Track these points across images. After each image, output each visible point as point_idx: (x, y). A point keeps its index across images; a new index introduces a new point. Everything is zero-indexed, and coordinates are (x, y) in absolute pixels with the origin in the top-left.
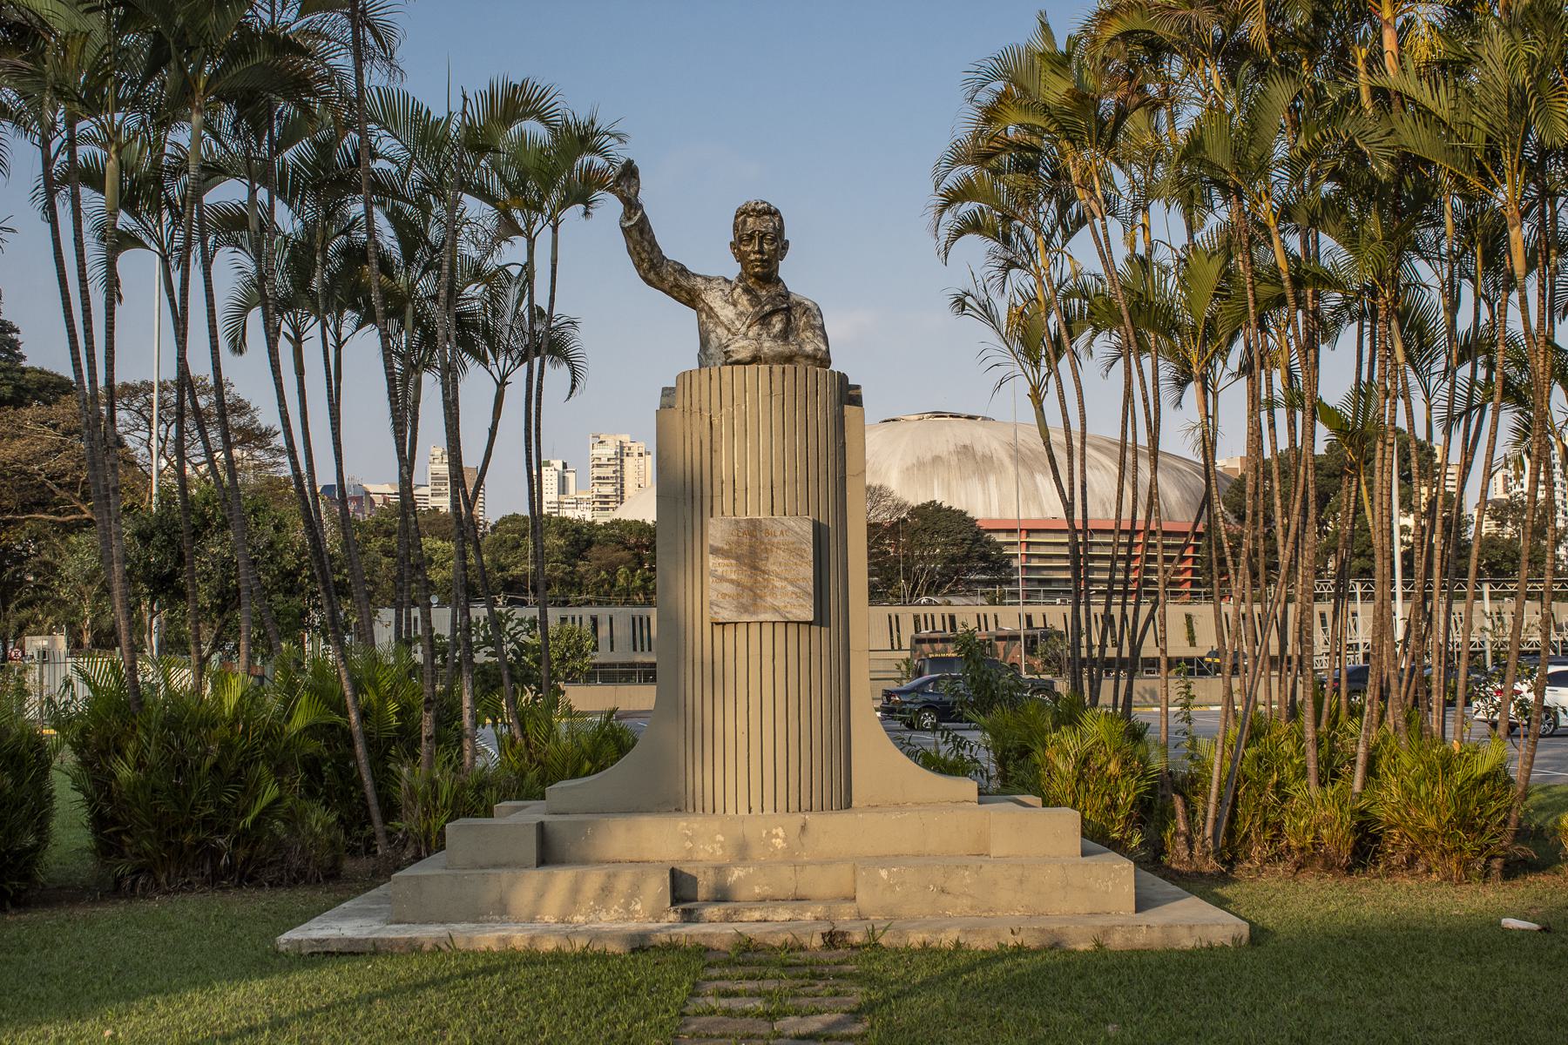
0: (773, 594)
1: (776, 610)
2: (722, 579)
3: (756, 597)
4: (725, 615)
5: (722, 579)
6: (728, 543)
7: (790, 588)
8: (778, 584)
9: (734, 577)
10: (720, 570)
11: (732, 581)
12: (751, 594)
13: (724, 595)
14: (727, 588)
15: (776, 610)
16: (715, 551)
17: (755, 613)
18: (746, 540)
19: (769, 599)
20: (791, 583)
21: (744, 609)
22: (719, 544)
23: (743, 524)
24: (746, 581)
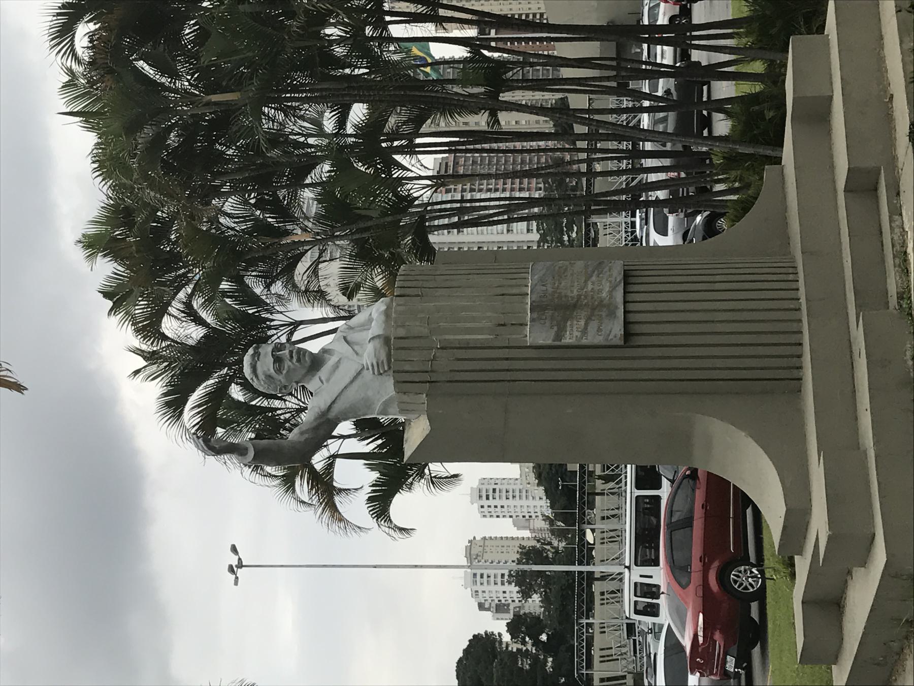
0: (600, 291)
1: (613, 288)
2: (584, 331)
3: (601, 305)
4: (617, 329)
5: (584, 331)
6: (552, 327)
7: (594, 278)
8: (590, 287)
9: (582, 323)
10: (576, 333)
11: (586, 324)
12: (597, 309)
13: (599, 330)
14: (593, 326)
15: (613, 288)
16: (559, 336)
17: (617, 308)
18: (549, 313)
19: (604, 295)
20: (591, 276)
21: (612, 314)
22: (552, 333)
23: (535, 315)
24: (584, 314)
